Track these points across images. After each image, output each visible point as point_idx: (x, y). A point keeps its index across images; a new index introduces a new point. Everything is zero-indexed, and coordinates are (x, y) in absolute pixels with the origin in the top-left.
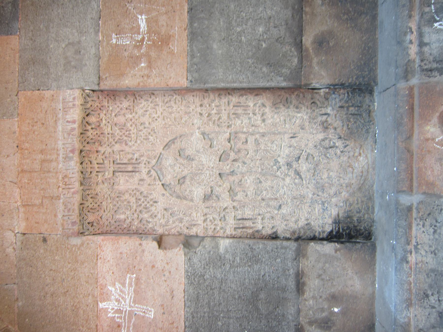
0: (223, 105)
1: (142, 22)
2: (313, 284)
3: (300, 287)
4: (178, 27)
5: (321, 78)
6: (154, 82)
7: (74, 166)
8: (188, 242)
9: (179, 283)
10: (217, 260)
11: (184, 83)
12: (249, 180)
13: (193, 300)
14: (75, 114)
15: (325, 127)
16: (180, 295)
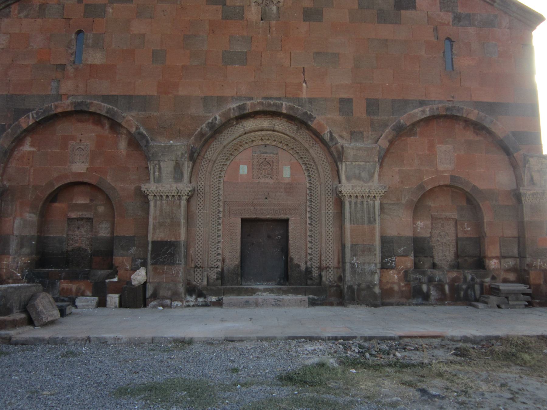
0: (454, 243)
1: (469, 229)
2: (426, 259)
3: (425, 257)
4: (467, 235)
5: (460, 260)
6: (458, 231)
7: (444, 217)
9: (424, 235)
10: (428, 242)
11: (459, 236)
12: (441, 248)
13: (421, 238)
14: (453, 217)
15: (451, 261)
16: (422, 236)
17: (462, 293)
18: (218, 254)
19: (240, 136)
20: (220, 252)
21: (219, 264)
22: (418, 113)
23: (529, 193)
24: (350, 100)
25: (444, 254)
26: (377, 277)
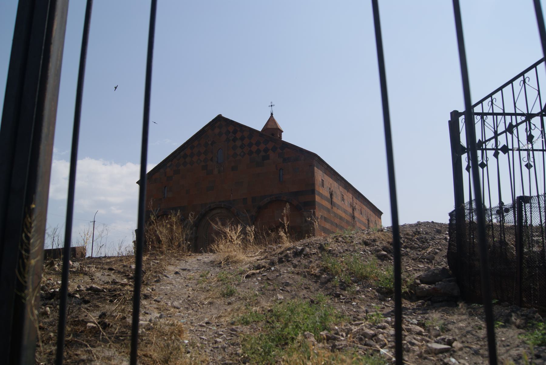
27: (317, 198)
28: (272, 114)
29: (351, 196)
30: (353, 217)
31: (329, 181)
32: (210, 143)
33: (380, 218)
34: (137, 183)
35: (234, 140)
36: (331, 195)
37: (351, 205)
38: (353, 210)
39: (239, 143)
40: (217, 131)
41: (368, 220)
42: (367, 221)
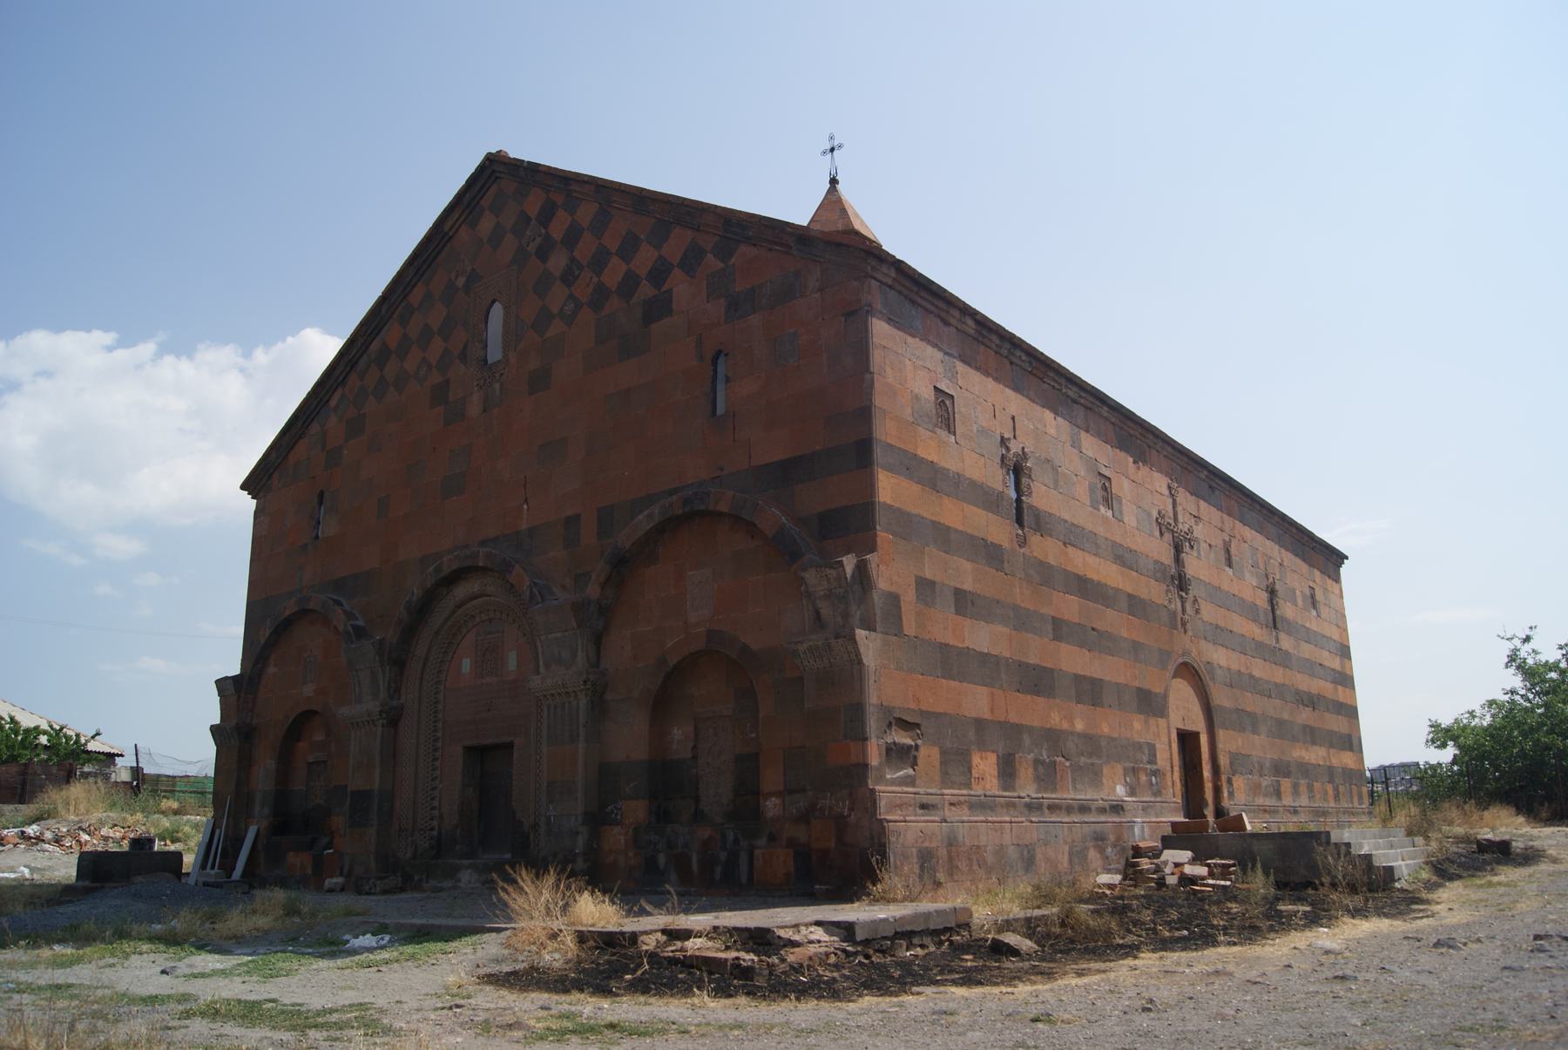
8: (695, 757)
17: (719, 870)
18: (433, 808)
19: (454, 612)
20: (436, 803)
21: (435, 823)
22: (644, 522)
23: (802, 648)
24: (578, 517)
25: (717, 791)
26: (581, 842)
27: (889, 488)
28: (834, 181)
29: (1160, 482)
30: (1181, 583)
31: (986, 399)
32: (461, 281)
33: (1337, 580)
34: (243, 487)
35: (543, 254)
36: (1018, 471)
37: (1163, 526)
38: (1178, 549)
39: (558, 262)
40: (486, 225)
41: (1272, 592)
42: (1265, 595)
